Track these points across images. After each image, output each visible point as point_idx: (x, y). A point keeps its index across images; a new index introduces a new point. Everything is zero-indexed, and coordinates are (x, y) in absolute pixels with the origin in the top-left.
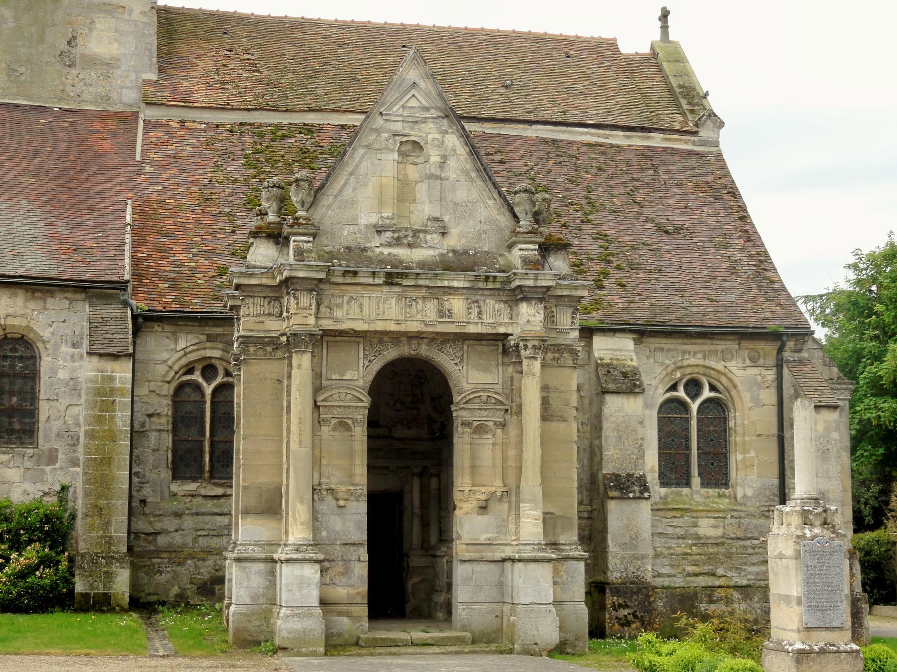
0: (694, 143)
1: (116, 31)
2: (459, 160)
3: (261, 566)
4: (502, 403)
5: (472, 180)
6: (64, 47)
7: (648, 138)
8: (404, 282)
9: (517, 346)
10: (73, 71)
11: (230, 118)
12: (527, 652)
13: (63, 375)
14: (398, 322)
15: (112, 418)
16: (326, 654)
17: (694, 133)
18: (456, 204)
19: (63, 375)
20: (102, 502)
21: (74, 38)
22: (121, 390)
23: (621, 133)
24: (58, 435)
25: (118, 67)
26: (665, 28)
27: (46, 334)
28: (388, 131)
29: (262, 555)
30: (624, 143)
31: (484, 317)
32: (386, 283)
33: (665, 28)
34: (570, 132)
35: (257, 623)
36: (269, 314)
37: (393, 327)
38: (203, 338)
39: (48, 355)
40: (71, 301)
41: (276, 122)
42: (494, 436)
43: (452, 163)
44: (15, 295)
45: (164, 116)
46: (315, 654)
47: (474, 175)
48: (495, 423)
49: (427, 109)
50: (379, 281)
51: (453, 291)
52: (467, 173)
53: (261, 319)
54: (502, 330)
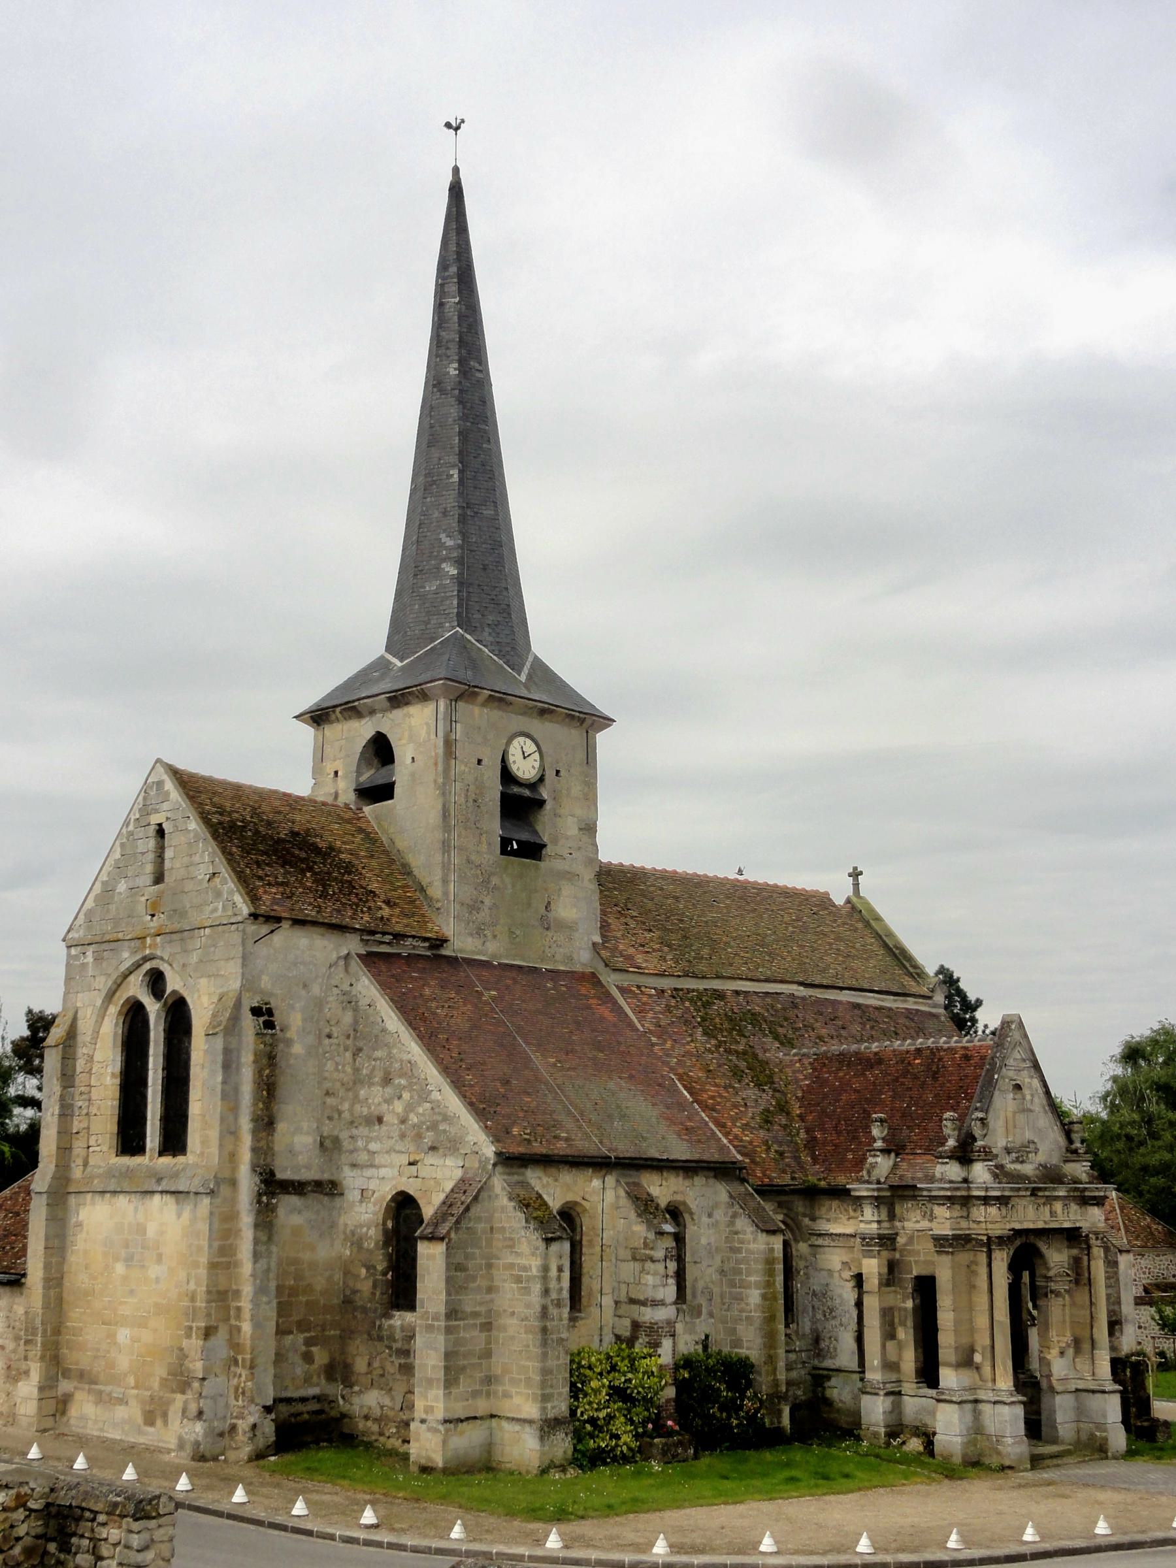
0: (929, 1006)
1: (575, 897)
2: (1039, 1097)
3: (969, 1407)
4: (1068, 1275)
5: (1046, 1112)
6: (543, 911)
7: (905, 1001)
8: (1040, 1194)
9: (1087, 1236)
10: (549, 934)
11: (666, 983)
12: (1115, 1458)
13: (704, 1241)
14: (1034, 1222)
15: (774, 1283)
16: (1032, 1470)
17: (930, 998)
18: (1040, 1130)
19: (704, 1241)
20: (772, 1352)
21: (549, 903)
22: (777, 1258)
23: (892, 997)
24: (702, 1292)
25: (577, 930)
26: (856, 885)
27: (693, 1206)
28: (1008, 1077)
29: (971, 1398)
30: (894, 1005)
31: (1070, 1215)
32: (1033, 1194)
33: (856, 885)
34: (864, 996)
35: (972, 1448)
36: (962, 1217)
37: (1031, 1226)
38: (776, 1204)
39: (694, 1225)
40: (707, 1178)
41: (695, 987)
42: (1064, 1299)
43: (1036, 1100)
44: (678, 1175)
45: (625, 981)
46: (1025, 1470)
47: (1047, 1108)
48: (1065, 1290)
49: (1024, 1060)
50: (1029, 1193)
51: (1057, 1198)
52: (1044, 1108)
53: (959, 1220)
54: (1078, 1225)
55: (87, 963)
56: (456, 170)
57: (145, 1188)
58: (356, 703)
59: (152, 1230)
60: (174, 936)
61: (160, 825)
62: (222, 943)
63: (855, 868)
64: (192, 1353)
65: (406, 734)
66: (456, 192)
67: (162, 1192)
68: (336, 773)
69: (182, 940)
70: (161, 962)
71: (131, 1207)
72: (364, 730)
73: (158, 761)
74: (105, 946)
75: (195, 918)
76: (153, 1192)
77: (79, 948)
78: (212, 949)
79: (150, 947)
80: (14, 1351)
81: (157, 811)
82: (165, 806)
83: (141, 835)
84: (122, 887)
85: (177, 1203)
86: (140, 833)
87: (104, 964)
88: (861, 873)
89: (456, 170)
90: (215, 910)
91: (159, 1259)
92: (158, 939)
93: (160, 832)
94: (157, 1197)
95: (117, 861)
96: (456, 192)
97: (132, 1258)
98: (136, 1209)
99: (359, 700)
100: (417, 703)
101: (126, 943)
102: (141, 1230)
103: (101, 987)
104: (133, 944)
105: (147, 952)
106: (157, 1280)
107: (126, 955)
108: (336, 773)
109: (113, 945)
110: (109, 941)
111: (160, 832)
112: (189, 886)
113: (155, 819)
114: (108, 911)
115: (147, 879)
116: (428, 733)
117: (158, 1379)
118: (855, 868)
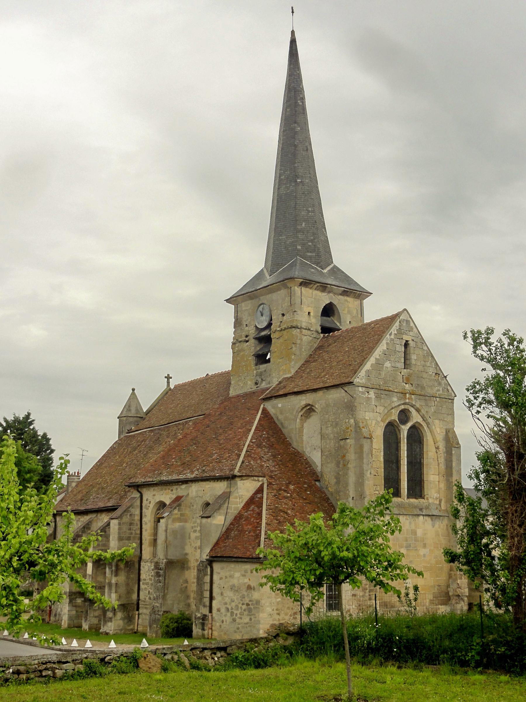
55: (371, 398)
56: (293, 32)
57: (416, 513)
58: (329, 286)
59: (419, 532)
60: (421, 397)
61: (407, 341)
62: (445, 406)
63: (168, 375)
64: (463, 586)
65: (346, 309)
66: (293, 42)
67: (423, 515)
68: (309, 313)
69: (426, 400)
70: (410, 407)
71: (408, 522)
72: (325, 299)
73: (405, 310)
74: (383, 392)
75: (429, 391)
76: (419, 515)
77: (364, 389)
78: (441, 408)
79: (409, 399)
80: (363, 596)
81: (406, 334)
82: (411, 333)
83: (398, 342)
84: (388, 364)
85: (432, 520)
86: (398, 342)
87: (382, 401)
88: (171, 378)
89: (293, 32)
90: (439, 390)
91: (425, 546)
92: (413, 396)
93: (406, 345)
94: (421, 518)
95: (384, 351)
96: (293, 42)
97: (410, 546)
98: (410, 523)
99: (331, 285)
100: (352, 297)
101: (395, 394)
102: (414, 532)
103: (381, 411)
104: (399, 395)
105: (407, 401)
106: (424, 556)
107: (395, 399)
108: (309, 313)
109: (387, 393)
110: (385, 390)
111: (406, 345)
112: (425, 375)
113: (405, 338)
114: (380, 374)
115: (401, 365)
116: (357, 313)
117: (428, 600)
118: (168, 375)
